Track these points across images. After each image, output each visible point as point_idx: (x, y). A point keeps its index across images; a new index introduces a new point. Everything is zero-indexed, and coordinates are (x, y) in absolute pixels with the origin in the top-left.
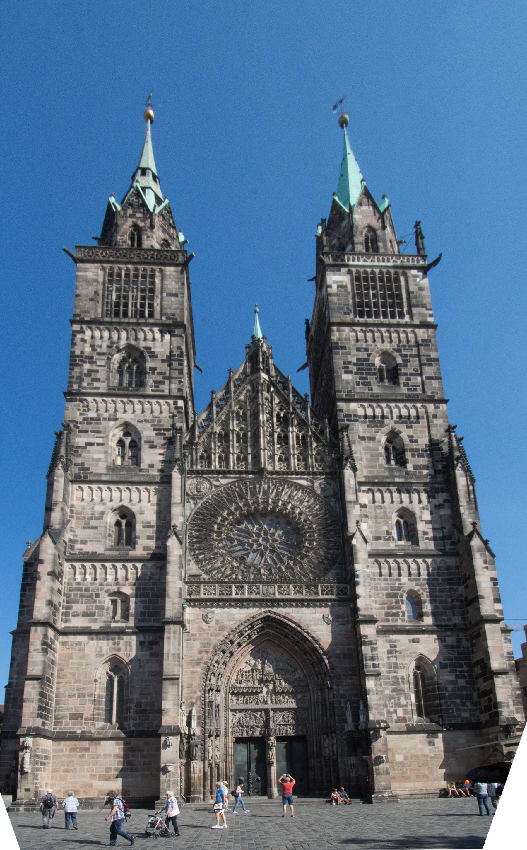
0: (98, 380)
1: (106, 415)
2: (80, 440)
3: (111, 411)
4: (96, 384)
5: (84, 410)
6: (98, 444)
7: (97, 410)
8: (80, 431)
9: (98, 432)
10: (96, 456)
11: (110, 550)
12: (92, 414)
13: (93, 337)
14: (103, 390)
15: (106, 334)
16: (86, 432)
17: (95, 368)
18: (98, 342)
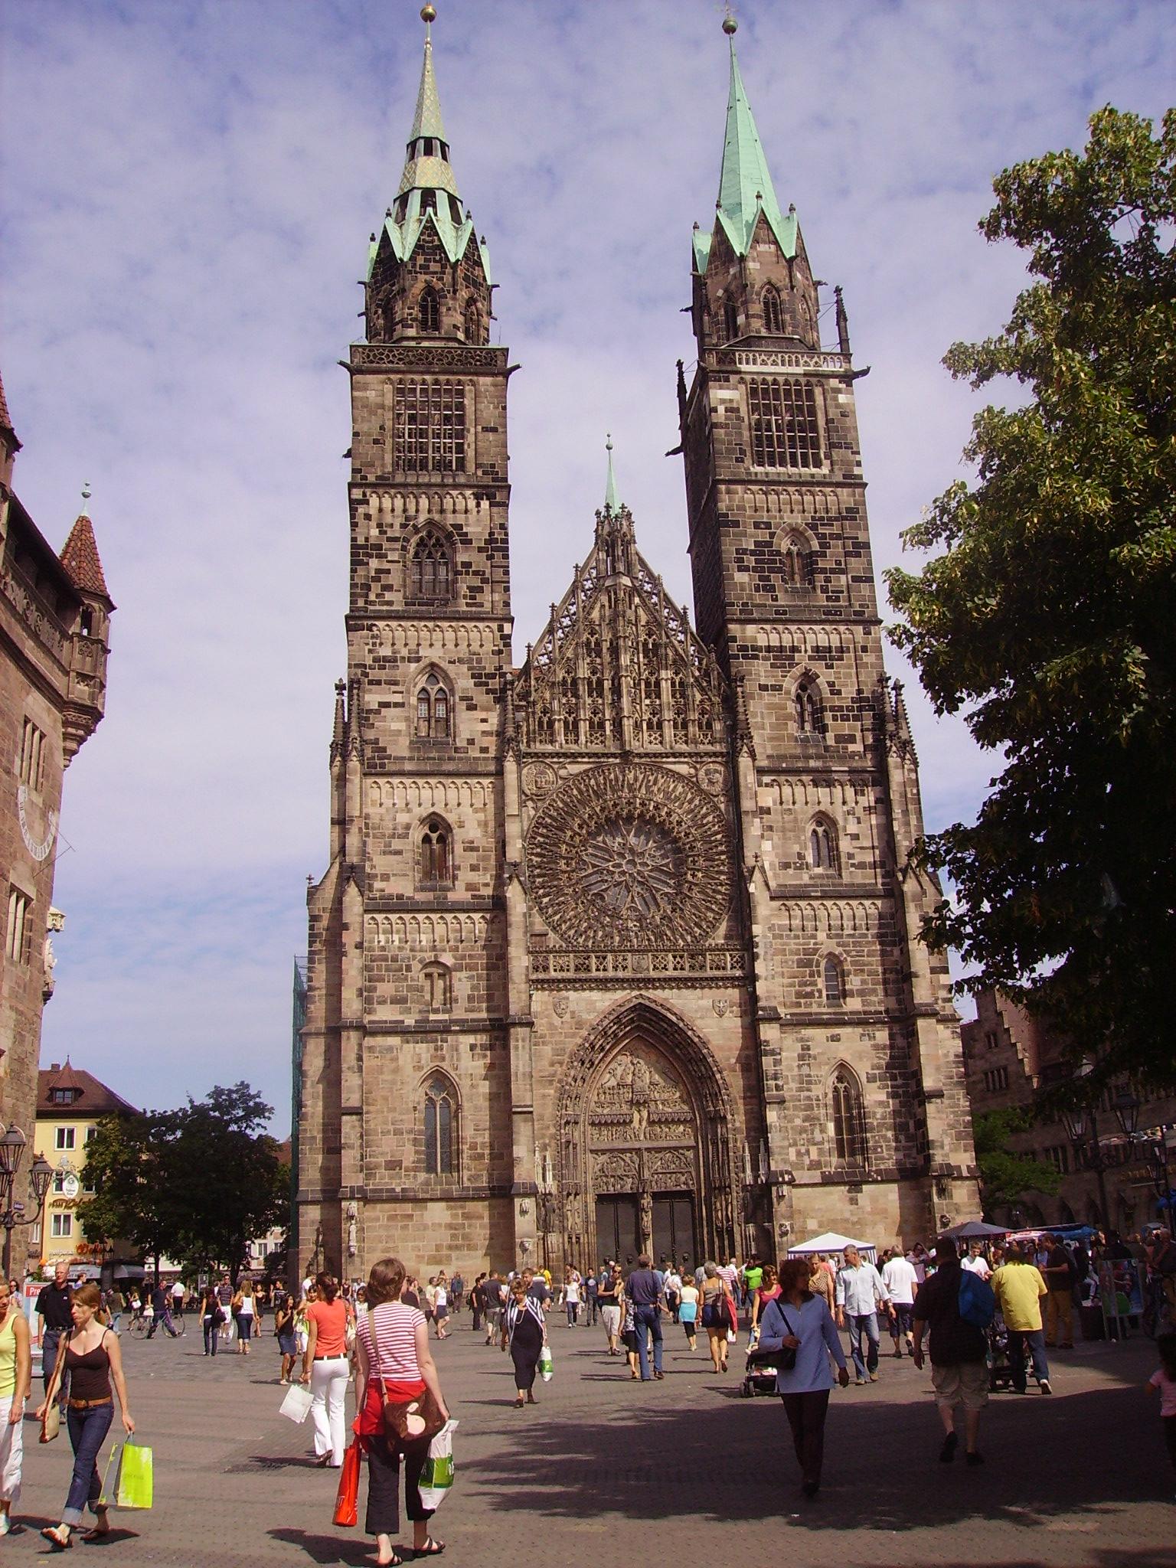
0: (388, 588)
1: (404, 652)
2: (372, 698)
3: (413, 646)
4: (388, 596)
5: (374, 644)
6: (397, 705)
7: (393, 644)
8: (371, 683)
9: (396, 683)
10: (395, 726)
11: (422, 889)
12: (385, 651)
13: (380, 510)
14: (398, 607)
15: (399, 502)
16: (379, 683)
17: (387, 566)
18: (388, 518)
